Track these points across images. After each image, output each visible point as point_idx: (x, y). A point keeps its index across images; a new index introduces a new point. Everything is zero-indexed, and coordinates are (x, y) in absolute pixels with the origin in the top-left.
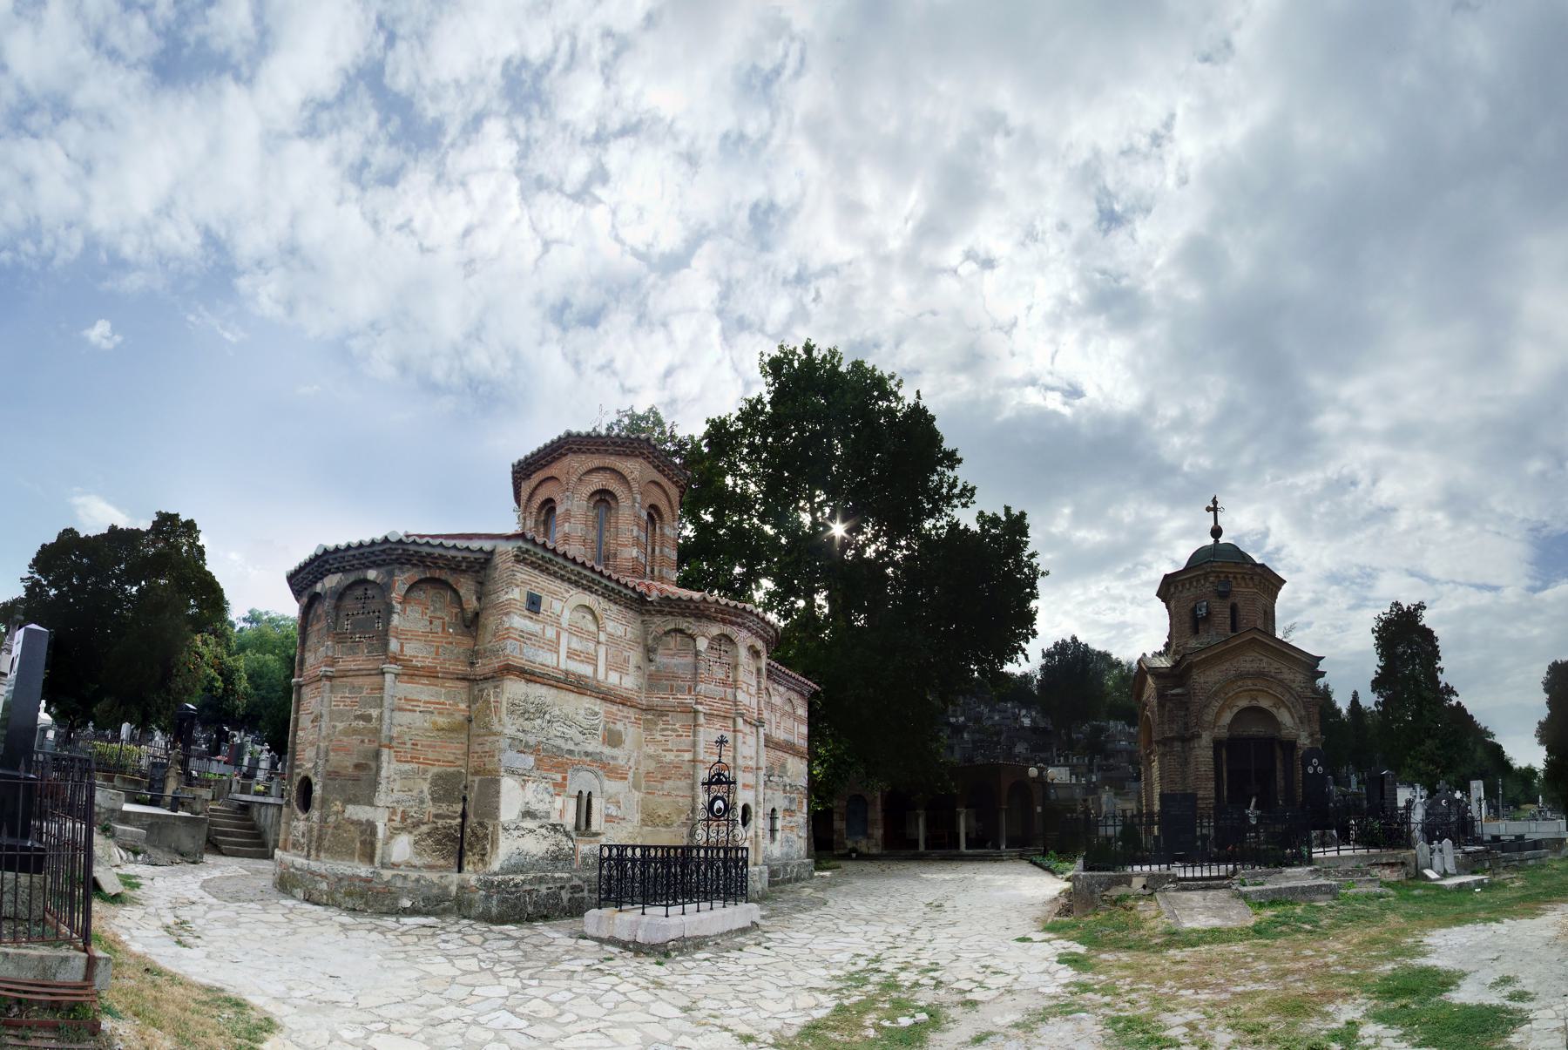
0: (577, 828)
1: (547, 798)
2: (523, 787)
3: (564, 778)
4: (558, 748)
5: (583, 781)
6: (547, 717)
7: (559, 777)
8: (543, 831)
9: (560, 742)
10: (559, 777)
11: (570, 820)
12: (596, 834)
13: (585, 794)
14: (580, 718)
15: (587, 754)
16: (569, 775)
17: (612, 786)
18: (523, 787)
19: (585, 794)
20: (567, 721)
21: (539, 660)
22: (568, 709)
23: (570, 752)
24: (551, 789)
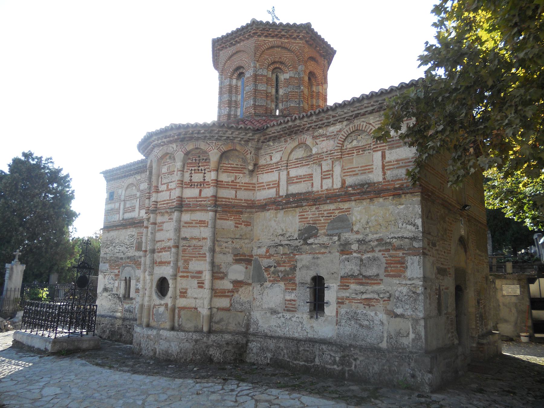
0: (124, 297)
1: (112, 281)
2: (104, 277)
3: (119, 272)
4: (117, 258)
5: (127, 271)
6: (114, 245)
7: (116, 271)
8: (110, 297)
9: (118, 255)
10: (116, 271)
11: (122, 291)
12: (132, 299)
13: (128, 278)
14: (126, 241)
15: (128, 258)
16: (120, 270)
17: (139, 273)
18: (104, 277)
19: (128, 278)
20: (121, 244)
21: (113, 220)
22: (122, 238)
23: (122, 258)
24: (114, 278)
